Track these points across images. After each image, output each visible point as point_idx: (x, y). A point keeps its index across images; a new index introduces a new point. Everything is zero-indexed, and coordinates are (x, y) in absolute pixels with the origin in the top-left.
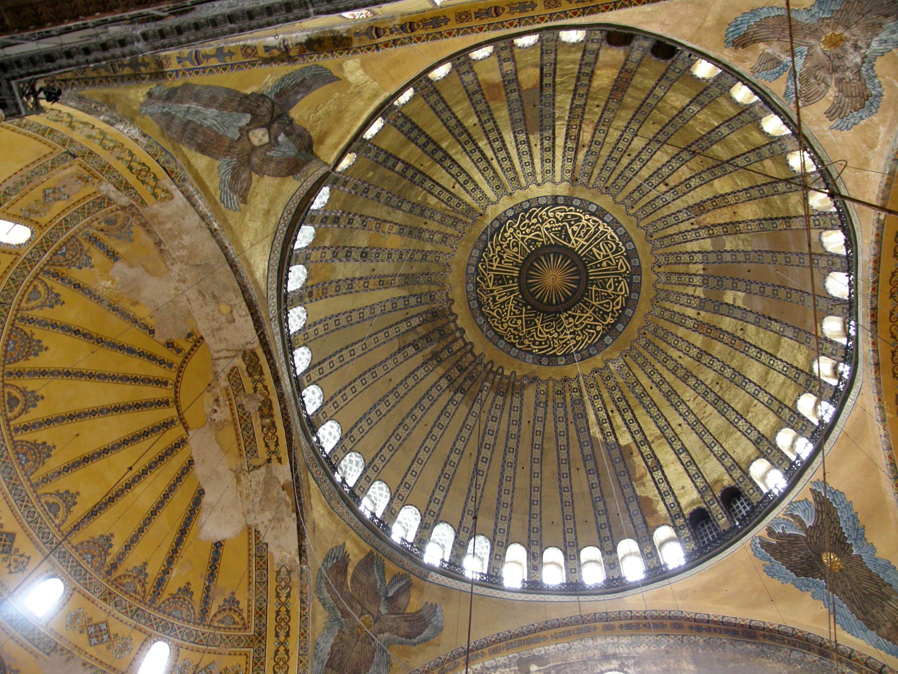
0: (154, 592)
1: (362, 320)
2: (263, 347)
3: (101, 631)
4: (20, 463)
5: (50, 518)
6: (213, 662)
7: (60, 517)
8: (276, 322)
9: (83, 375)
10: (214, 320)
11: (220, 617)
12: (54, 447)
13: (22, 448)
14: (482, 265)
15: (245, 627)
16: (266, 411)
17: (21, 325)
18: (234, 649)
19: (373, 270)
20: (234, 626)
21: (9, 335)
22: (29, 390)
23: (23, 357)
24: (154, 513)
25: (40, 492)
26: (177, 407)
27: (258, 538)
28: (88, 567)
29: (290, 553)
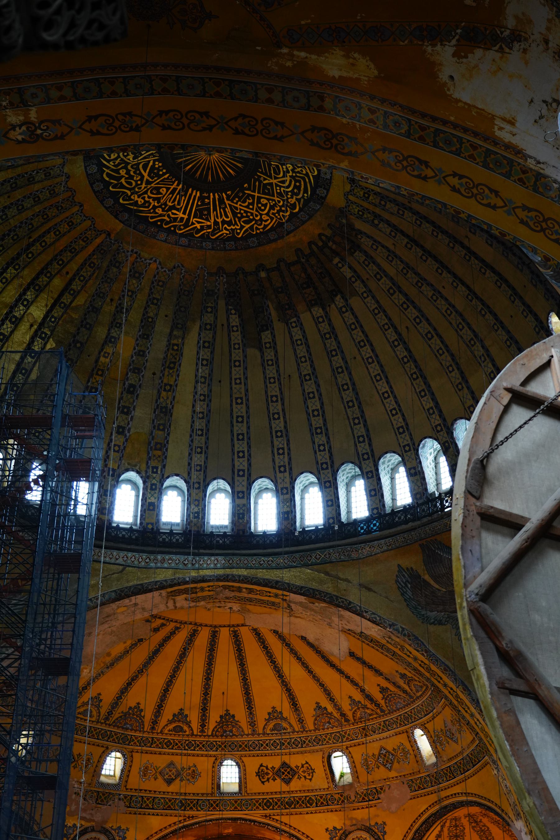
1: (207, 398)
2: (167, 588)
4: (231, 736)
8: (152, 557)
11: (414, 689)
12: (227, 711)
14: (181, 230)
15: (427, 687)
17: (112, 720)
19: (154, 374)
21: (118, 727)
22: (171, 718)
23: (140, 719)
24: (310, 672)
25: (261, 731)
26: (220, 626)
28: (335, 730)
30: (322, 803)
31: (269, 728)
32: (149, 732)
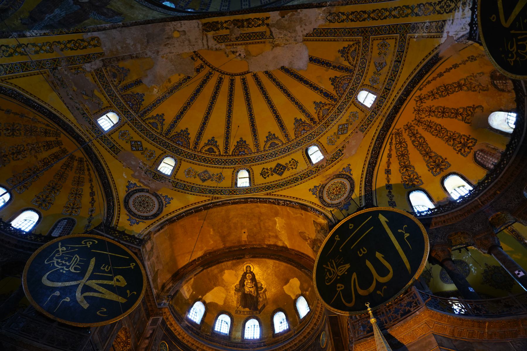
0: (331, 99)
2: (201, 18)
3: (342, 128)
4: (244, 155)
5: (277, 147)
6: (374, 63)
7: (279, 143)
9: (207, 117)
10: (183, 42)
11: (351, 59)
12: (241, 138)
13: (236, 152)
15: (358, 43)
16: (240, 24)
17: (169, 136)
18: (369, 49)
20: (357, 50)
21: (174, 142)
22: (207, 142)
23: (188, 140)
24: (289, 95)
25: (262, 150)
26: (235, 75)
27: (310, 35)
28: (308, 133)
29: (320, 14)
30: (305, 177)
31: (267, 147)
32: (193, 150)
